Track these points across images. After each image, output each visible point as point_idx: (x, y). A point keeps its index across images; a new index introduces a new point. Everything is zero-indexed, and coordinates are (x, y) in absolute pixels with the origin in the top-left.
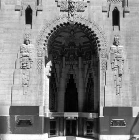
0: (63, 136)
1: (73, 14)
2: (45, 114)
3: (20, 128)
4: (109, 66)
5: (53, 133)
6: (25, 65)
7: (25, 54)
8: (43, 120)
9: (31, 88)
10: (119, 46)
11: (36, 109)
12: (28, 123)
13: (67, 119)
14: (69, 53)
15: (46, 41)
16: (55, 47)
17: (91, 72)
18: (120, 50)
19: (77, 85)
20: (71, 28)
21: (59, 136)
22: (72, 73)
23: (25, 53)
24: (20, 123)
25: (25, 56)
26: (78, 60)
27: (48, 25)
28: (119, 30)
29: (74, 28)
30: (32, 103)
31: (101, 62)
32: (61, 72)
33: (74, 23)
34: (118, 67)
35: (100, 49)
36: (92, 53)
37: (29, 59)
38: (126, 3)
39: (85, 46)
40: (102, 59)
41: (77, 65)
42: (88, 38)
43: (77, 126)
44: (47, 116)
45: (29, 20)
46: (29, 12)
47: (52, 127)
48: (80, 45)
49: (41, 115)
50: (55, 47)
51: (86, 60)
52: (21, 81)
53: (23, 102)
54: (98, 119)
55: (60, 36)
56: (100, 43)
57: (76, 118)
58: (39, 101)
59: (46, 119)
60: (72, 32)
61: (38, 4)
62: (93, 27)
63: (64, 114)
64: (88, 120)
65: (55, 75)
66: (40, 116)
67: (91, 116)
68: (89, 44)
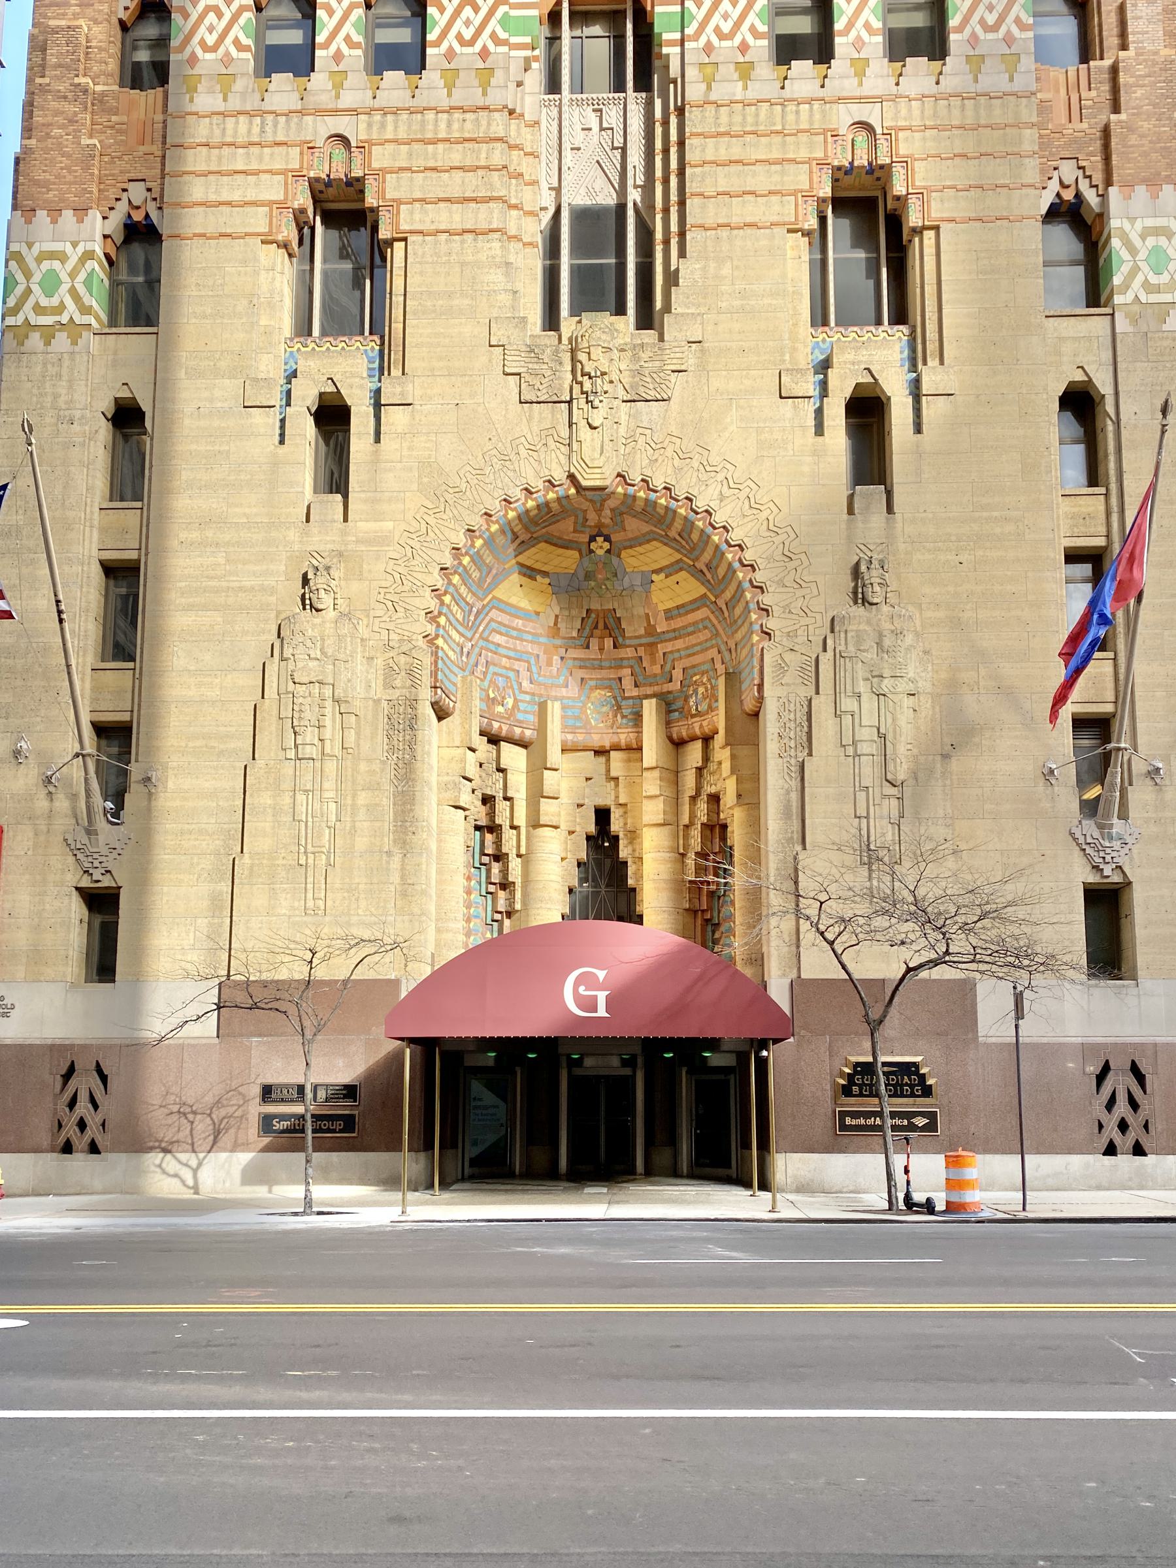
16: (497, 638)
26: (638, 718)
28: (890, 509)
37: (337, 701)
38: (932, 347)
39: (677, 634)
42: (698, 574)
46: (332, 416)
48: (650, 630)
50: (497, 638)
62: (722, 497)
65: (502, 806)
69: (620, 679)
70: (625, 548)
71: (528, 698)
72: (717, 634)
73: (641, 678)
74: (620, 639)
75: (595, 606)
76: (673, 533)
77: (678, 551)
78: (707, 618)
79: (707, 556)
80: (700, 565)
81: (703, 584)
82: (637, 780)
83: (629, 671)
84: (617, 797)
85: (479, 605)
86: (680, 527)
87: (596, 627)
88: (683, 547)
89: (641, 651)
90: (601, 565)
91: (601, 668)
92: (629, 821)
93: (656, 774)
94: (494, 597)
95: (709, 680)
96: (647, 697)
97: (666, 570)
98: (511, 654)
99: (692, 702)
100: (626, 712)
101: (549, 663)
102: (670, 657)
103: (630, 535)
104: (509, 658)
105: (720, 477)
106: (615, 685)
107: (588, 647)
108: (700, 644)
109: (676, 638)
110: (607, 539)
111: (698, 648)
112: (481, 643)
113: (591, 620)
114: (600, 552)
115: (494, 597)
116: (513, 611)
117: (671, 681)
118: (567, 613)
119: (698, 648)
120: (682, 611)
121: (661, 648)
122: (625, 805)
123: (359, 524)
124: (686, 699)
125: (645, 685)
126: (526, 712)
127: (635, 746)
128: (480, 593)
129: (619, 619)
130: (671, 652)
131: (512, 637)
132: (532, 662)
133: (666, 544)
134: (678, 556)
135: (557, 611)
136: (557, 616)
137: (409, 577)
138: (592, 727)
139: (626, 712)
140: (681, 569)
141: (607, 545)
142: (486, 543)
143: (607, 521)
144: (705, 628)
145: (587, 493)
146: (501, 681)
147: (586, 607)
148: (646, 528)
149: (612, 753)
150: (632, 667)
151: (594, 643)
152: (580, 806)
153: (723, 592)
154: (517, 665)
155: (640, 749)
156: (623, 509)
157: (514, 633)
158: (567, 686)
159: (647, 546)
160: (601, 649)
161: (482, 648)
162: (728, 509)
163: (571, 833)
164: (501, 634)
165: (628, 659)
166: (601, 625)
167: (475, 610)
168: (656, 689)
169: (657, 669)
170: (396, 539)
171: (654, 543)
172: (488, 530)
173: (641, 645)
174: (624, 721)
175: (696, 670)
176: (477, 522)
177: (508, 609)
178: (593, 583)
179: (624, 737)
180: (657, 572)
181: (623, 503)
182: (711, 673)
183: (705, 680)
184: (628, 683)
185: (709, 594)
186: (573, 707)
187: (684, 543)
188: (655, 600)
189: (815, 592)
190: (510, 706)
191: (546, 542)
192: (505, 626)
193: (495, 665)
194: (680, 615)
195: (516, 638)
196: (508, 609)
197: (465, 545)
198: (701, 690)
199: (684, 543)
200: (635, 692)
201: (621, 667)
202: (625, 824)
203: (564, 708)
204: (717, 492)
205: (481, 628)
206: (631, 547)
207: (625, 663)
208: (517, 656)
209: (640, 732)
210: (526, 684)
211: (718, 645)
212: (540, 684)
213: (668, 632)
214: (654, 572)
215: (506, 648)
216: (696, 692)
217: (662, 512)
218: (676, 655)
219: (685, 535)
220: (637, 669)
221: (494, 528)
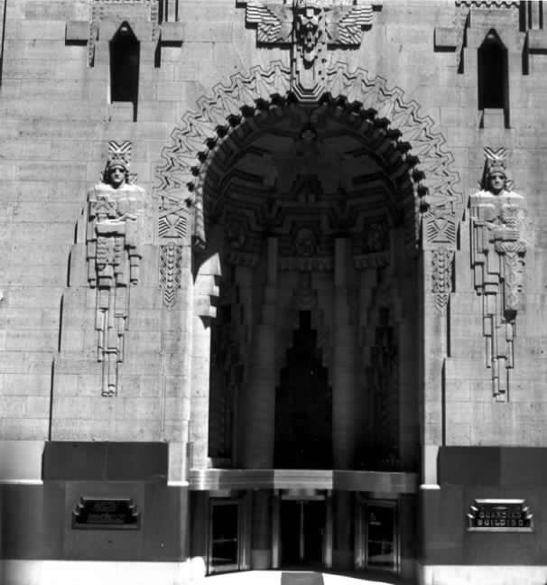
0: (270, 568)
1: (310, 56)
2: (192, 477)
3: (90, 535)
4: (465, 277)
5: (224, 557)
6: (108, 271)
7: (106, 225)
8: (184, 500)
9: (134, 365)
10: (505, 194)
11: (158, 453)
12: (122, 513)
13: (284, 497)
14: (294, 223)
15: (195, 171)
16: (234, 195)
18: (512, 211)
19: (325, 356)
20: (304, 119)
21: (251, 568)
22: (305, 308)
23: (108, 222)
24: (89, 514)
25: (108, 235)
27: (204, 105)
28: (507, 125)
29: (314, 119)
30: (138, 429)
31: (428, 258)
32: (259, 303)
33: (318, 94)
34: (502, 280)
35: (424, 207)
36: (390, 221)
37: (127, 247)
40: (435, 246)
41: (331, 272)
42: (378, 160)
43: (329, 526)
44: (202, 486)
45: (125, 86)
47: (220, 531)
48: (342, 191)
49: (177, 480)
50: (234, 195)
51: (367, 251)
52: (92, 338)
53: (100, 426)
54: (416, 499)
55: (259, 152)
56: (424, 183)
57: (324, 492)
58: (169, 423)
59: (195, 496)
60: (308, 136)
61: (161, 15)
62: (394, 112)
63: (271, 476)
64: (370, 503)
66: (170, 483)
67: (386, 485)
68: (377, 183)
80: (377, 153)
85: (222, 175)
105: (393, 99)
110: (314, 131)
114: (309, 139)
121: (350, 203)
123: (145, 123)
141: (313, 136)
151: (302, 198)
162: (399, 121)
170: (170, 133)
189: (457, 180)
204: (391, 110)
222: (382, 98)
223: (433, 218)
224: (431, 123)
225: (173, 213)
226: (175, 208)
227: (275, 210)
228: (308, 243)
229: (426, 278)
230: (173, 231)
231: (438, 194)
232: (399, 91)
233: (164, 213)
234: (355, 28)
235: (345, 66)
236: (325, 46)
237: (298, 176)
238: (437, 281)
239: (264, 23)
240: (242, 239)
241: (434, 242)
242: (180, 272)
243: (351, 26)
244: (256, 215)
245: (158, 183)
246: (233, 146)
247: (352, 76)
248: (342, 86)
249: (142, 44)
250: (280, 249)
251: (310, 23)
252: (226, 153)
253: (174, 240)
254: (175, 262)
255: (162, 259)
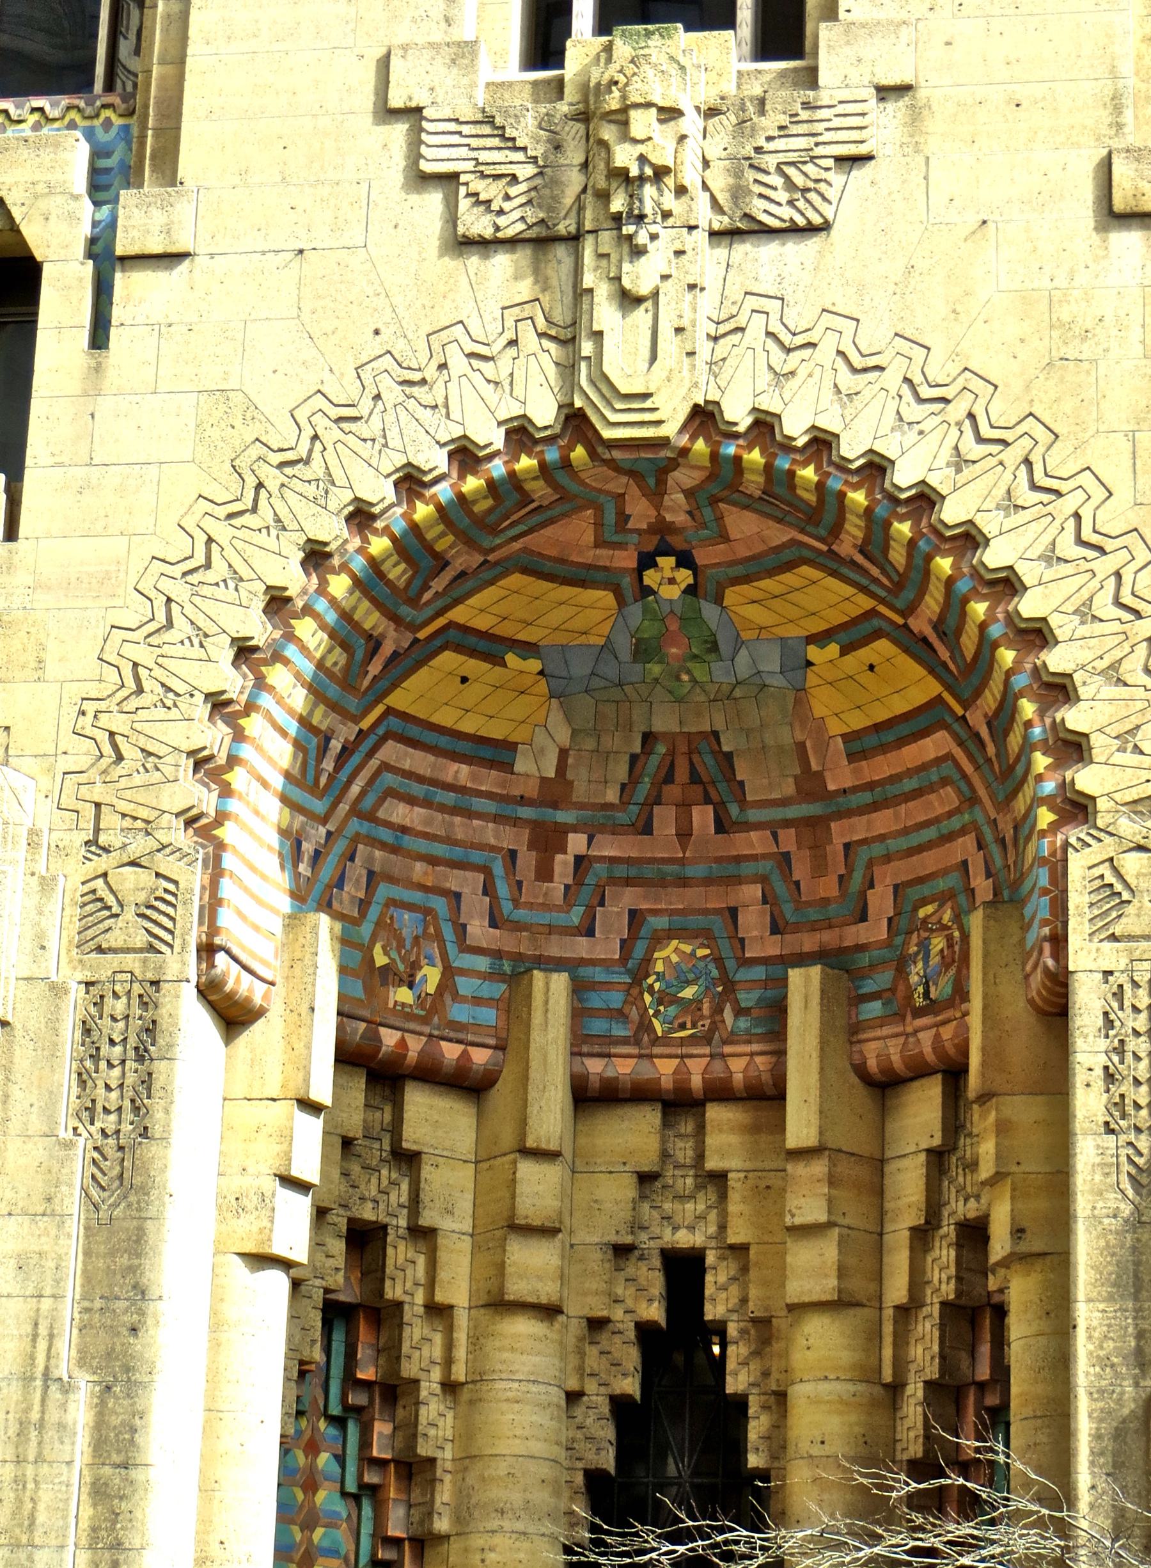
14: (636, 917)
16: (399, 813)
17: (971, 1210)
19: (757, 1427)
22: (684, 1239)
26: (774, 1018)
31: (1088, 1001)
35: (1077, 808)
36: (982, 886)
39: (880, 795)
40: (1113, 956)
41: (768, 1096)
42: (917, 647)
48: (810, 785)
51: (902, 1008)
55: (489, 647)
62: (960, 462)
69: (733, 912)
70: (736, 581)
71: (482, 963)
72: (973, 800)
73: (788, 910)
74: (734, 810)
75: (664, 721)
76: (846, 547)
77: (863, 589)
78: (949, 757)
79: (932, 603)
80: (920, 624)
81: (932, 671)
82: (774, 1180)
83: (756, 891)
84: (722, 1227)
85: (346, 732)
86: (860, 534)
87: (669, 779)
88: (875, 580)
89: (789, 839)
90: (674, 626)
91: (684, 882)
92: (753, 1293)
93: (819, 1168)
94: (389, 711)
95: (957, 918)
96: (801, 960)
97: (844, 637)
98: (439, 850)
99: (916, 972)
100: (747, 998)
101: (545, 873)
102: (863, 855)
103: (743, 552)
104: (433, 861)
106: (718, 925)
107: (647, 829)
108: (936, 821)
109: (875, 807)
110: (685, 560)
111: (930, 833)
112: (355, 825)
113: (654, 760)
114: (671, 593)
115: (389, 711)
116: (444, 741)
117: (863, 918)
118: (589, 744)
119: (930, 833)
120: (889, 737)
121: (840, 833)
122: (741, 1250)
124: (902, 966)
125: (797, 928)
126: (477, 1001)
127: (771, 1091)
128: (352, 703)
129: (729, 756)
130: (864, 842)
131: (442, 808)
132: (498, 869)
133: (834, 574)
134: (865, 603)
135: (563, 735)
136: (563, 753)
137: (158, 672)
138: (656, 1041)
139: (747, 998)
140: (877, 635)
142: (358, 583)
143: (677, 517)
144: (945, 781)
145: (617, 454)
146: (408, 923)
147: (640, 728)
148: (779, 535)
149: (715, 1113)
150: (764, 880)
151: (665, 820)
152: (622, 1252)
153: (978, 692)
154: (455, 880)
155: (781, 1097)
156: (714, 489)
157: (450, 798)
158: (590, 933)
159: (788, 578)
160: (684, 834)
161: (356, 839)
163: (596, 1324)
164: (411, 801)
165: (754, 858)
166: (682, 773)
167: (336, 745)
168: (828, 937)
169: (828, 887)
171: (805, 570)
172: (361, 551)
173: (787, 823)
174: (743, 1023)
175: (925, 890)
176: (331, 529)
177: (430, 737)
178: (656, 669)
179: (742, 1065)
180: (819, 639)
181: (712, 477)
182: (962, 899)
183: (947, 916)
184: (753, 922)
185: (947, 696)
186: (607, 986)
187: (875, 571)
188: (819, 710)
190: (431, 988)
191: (525, 571)
192: (421, 779)
193: (391, 880)
194: (884, 748)
195: (454, 811)
196: (430, 737)
197: (304, 591)
198: (938, 943)
199: (875, 571)
200: (773, 947)
201: (737, 880)
202: (744, 1301)
203: (579, 988)
204: (946, 454)
205: (355, 789)
206: (746, 579)
207: (747, 869)
208: (458, 853)
209: (780, 1054)
210: (478, 930)
211: (974, 827)
212: (518, 927)
213: (855, 789)
214: (811, 639)
215: (426, 836)
216: (924, 946)
217: (812, 498)
218: (878, 850)
219: (877, 553)
220: (780, 888)
221: (379, 545)
222: (914, 411)
223: (1109, 847)
224: (1099, 494)
225: (133, 863)
226: (139, 846)
227: (563, 864)
228: (688, 993)
229: (1080, 1077)
230: (128, 930)
231: (1129, 758)
232: (976, 384)
233: (103, 863)
234: (809, 168)
235: (773, 306)
236: (701, 236)
237: (648, 738)
238: (1126, 1088)
239: (483, 176)
240: (431, 976)
241: (1113, 938)
242: (148, 1080)
243: (792, 164)
244: (488, 889)
245: (80, 754)
246: (371, 619)
247: (799, 340)
248: (766, 377)
249: (47, 272)
250: (579, 1014)
251: (642, 159)
252: (345, 645)
253: (131, 961)
254: (132, 1041)
255: (87, 1032)
